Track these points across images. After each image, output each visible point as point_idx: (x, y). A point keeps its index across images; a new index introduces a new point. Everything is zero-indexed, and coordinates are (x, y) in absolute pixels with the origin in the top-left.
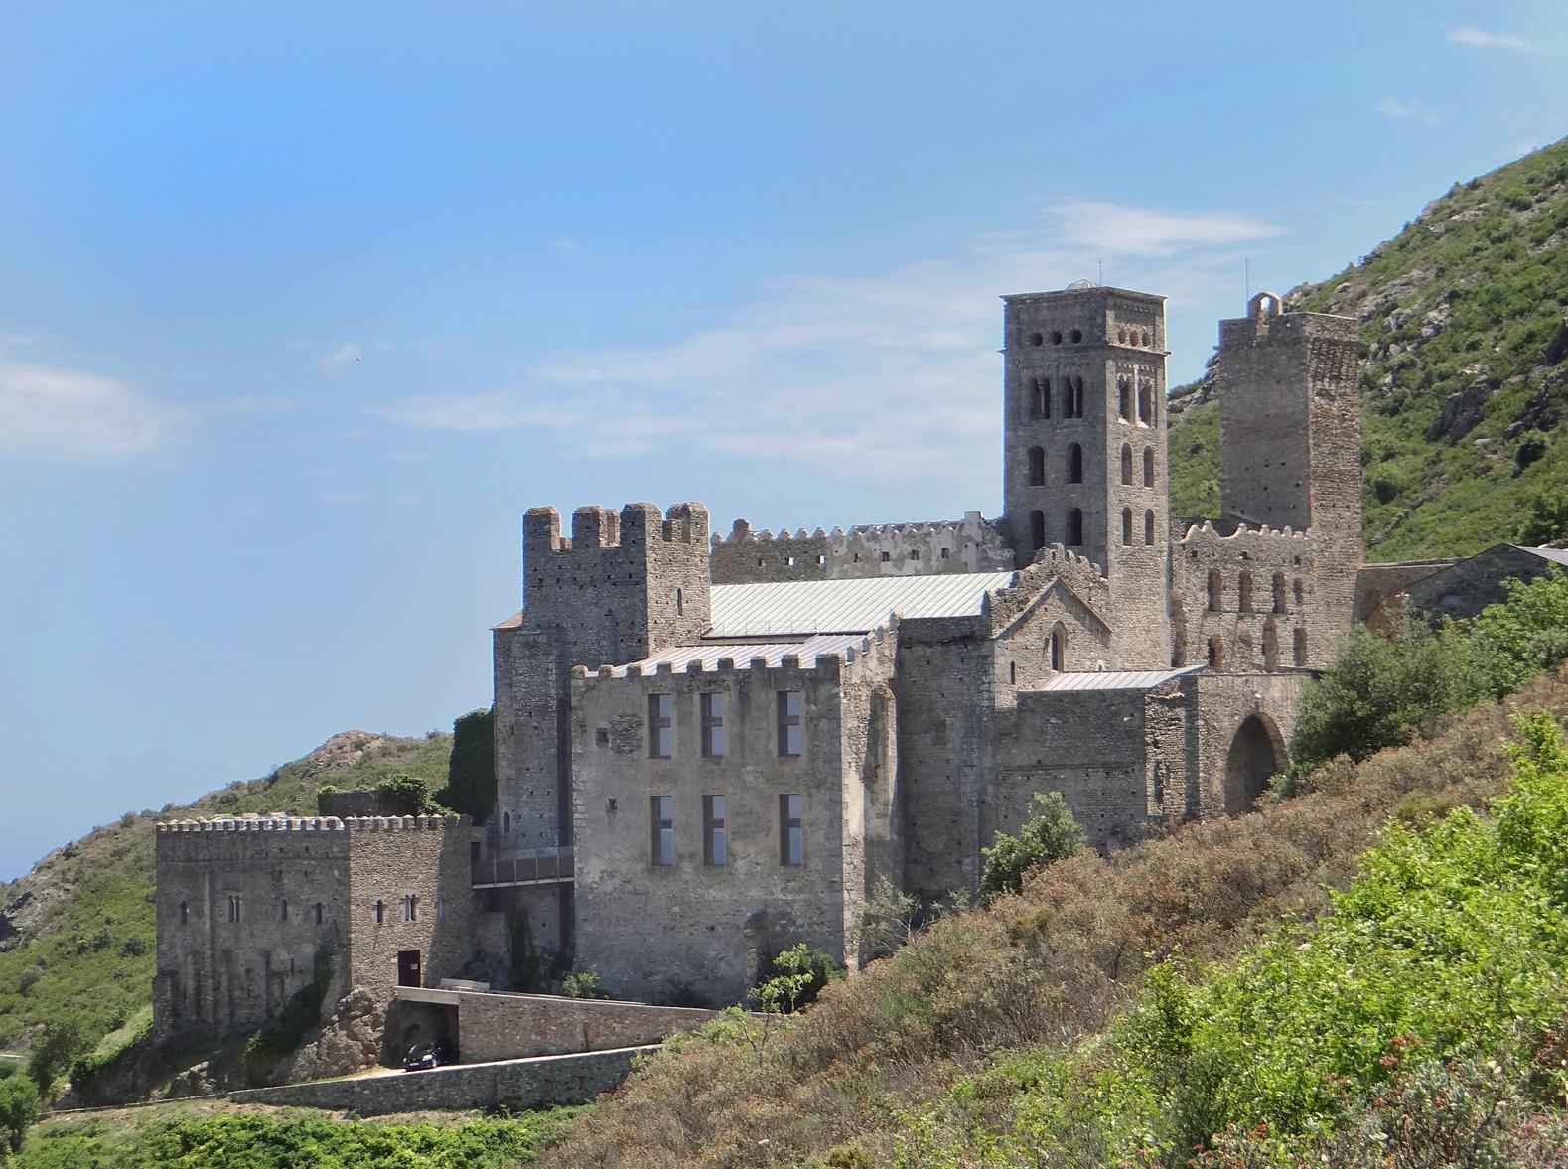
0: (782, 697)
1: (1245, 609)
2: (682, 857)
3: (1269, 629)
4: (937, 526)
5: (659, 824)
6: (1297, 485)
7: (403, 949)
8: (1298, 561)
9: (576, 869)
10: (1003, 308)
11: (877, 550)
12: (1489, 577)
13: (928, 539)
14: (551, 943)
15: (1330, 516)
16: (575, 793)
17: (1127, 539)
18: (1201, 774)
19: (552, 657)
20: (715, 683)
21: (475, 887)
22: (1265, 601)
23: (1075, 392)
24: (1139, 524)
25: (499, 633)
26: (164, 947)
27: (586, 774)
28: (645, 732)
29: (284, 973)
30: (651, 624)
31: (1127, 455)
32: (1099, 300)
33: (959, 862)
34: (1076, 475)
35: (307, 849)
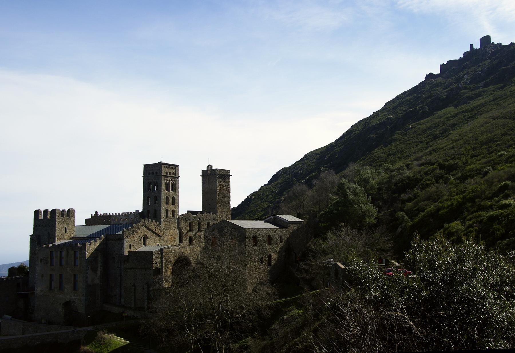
0: (75, 252)
5: (51, 280)
6: (215, 204)
10: (143, 167)
12: (221, 227)
13: (129, 216)
15: (223, 210)
17: (167, 216)
18: (164, 271)
19: (37, 242)
20: (62, 249)
21: (18, 293)
24: (170, 214)
25: (31, 236)
28: (49, 260)
30: (56, 235)
31: (167, 198)
32: (160, 164)
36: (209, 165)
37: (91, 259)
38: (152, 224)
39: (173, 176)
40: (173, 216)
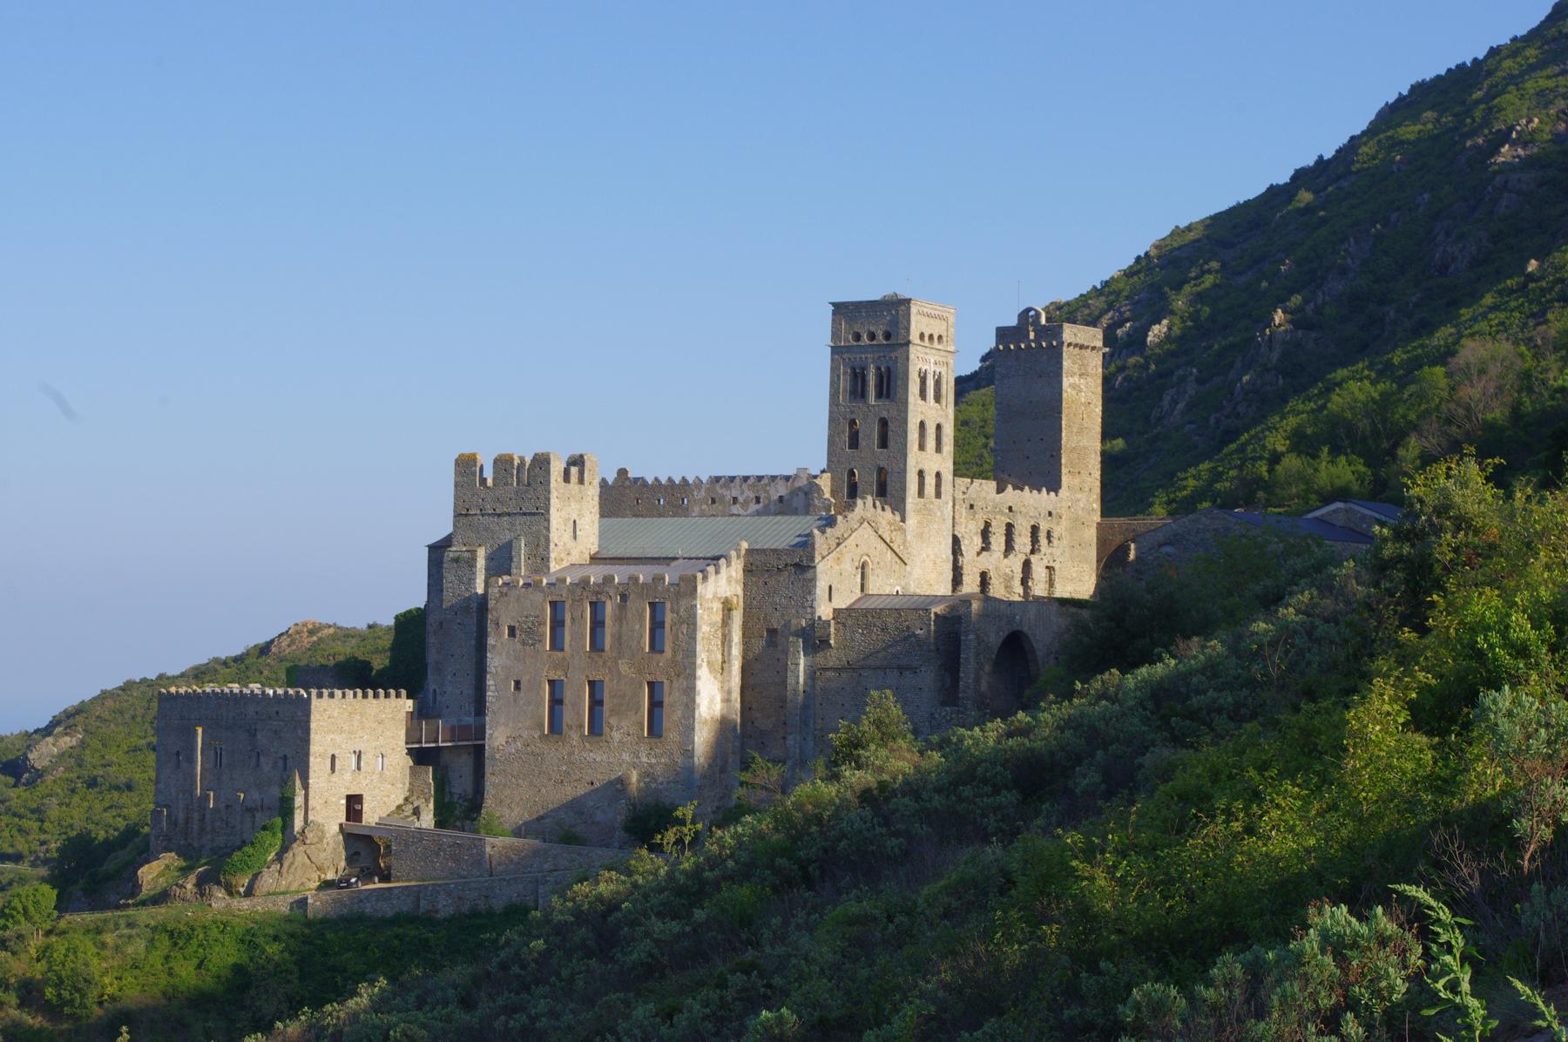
1: (1009, 547)
2: (570, 727)
3: (1027, 565)
4: (774, 478)
5: (556, 702)
6: (1052, 456)
7: (349, 793)
8: (1050, 514)
9: (487, 735)
11: (728, 495)
12: (1197, 532)
13: (768, 488)
14: (465, 791)
15: (1077, 481)
16: (488, 676)
17: (921, 493)
22: (1025, 544)
23: (885, 380)
24: (930, 481)
26: (161, 786)
27: (494, 662)
29: (256, 809)
30: (552, 546)
33: (784, 738)
34: (884, 443)
35: (277, 713)
36: (1029, 310)
37: (708, 629)
38: (887, 517)
39: (940, 347)
40: (938, 495)
